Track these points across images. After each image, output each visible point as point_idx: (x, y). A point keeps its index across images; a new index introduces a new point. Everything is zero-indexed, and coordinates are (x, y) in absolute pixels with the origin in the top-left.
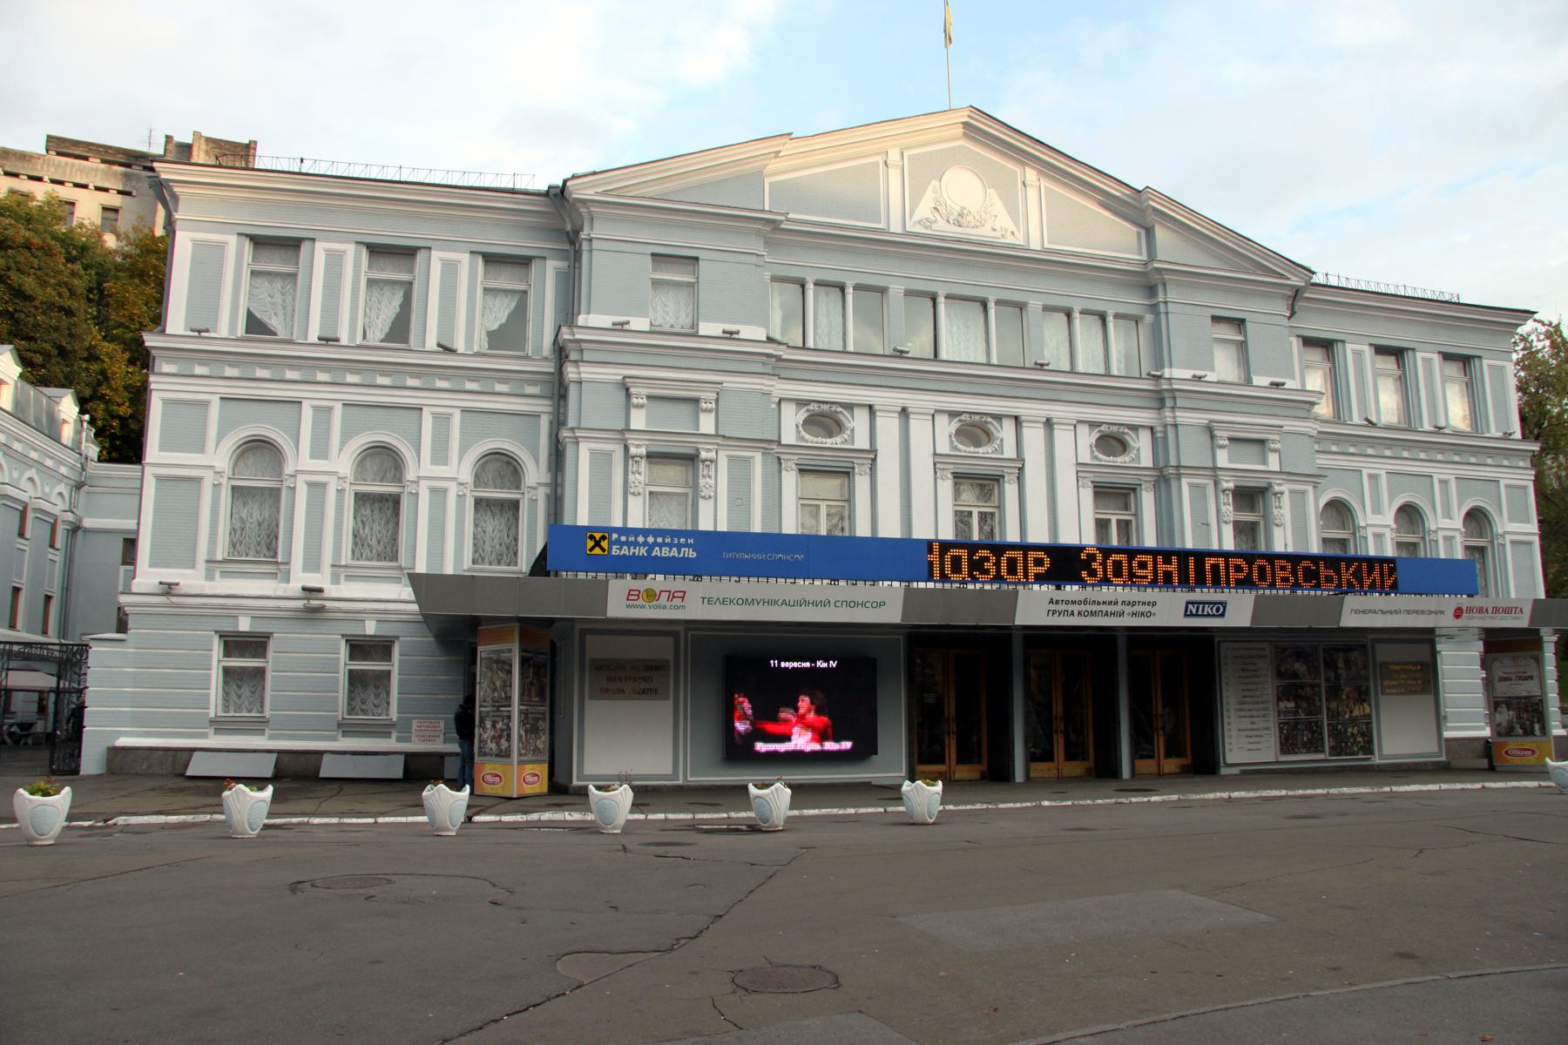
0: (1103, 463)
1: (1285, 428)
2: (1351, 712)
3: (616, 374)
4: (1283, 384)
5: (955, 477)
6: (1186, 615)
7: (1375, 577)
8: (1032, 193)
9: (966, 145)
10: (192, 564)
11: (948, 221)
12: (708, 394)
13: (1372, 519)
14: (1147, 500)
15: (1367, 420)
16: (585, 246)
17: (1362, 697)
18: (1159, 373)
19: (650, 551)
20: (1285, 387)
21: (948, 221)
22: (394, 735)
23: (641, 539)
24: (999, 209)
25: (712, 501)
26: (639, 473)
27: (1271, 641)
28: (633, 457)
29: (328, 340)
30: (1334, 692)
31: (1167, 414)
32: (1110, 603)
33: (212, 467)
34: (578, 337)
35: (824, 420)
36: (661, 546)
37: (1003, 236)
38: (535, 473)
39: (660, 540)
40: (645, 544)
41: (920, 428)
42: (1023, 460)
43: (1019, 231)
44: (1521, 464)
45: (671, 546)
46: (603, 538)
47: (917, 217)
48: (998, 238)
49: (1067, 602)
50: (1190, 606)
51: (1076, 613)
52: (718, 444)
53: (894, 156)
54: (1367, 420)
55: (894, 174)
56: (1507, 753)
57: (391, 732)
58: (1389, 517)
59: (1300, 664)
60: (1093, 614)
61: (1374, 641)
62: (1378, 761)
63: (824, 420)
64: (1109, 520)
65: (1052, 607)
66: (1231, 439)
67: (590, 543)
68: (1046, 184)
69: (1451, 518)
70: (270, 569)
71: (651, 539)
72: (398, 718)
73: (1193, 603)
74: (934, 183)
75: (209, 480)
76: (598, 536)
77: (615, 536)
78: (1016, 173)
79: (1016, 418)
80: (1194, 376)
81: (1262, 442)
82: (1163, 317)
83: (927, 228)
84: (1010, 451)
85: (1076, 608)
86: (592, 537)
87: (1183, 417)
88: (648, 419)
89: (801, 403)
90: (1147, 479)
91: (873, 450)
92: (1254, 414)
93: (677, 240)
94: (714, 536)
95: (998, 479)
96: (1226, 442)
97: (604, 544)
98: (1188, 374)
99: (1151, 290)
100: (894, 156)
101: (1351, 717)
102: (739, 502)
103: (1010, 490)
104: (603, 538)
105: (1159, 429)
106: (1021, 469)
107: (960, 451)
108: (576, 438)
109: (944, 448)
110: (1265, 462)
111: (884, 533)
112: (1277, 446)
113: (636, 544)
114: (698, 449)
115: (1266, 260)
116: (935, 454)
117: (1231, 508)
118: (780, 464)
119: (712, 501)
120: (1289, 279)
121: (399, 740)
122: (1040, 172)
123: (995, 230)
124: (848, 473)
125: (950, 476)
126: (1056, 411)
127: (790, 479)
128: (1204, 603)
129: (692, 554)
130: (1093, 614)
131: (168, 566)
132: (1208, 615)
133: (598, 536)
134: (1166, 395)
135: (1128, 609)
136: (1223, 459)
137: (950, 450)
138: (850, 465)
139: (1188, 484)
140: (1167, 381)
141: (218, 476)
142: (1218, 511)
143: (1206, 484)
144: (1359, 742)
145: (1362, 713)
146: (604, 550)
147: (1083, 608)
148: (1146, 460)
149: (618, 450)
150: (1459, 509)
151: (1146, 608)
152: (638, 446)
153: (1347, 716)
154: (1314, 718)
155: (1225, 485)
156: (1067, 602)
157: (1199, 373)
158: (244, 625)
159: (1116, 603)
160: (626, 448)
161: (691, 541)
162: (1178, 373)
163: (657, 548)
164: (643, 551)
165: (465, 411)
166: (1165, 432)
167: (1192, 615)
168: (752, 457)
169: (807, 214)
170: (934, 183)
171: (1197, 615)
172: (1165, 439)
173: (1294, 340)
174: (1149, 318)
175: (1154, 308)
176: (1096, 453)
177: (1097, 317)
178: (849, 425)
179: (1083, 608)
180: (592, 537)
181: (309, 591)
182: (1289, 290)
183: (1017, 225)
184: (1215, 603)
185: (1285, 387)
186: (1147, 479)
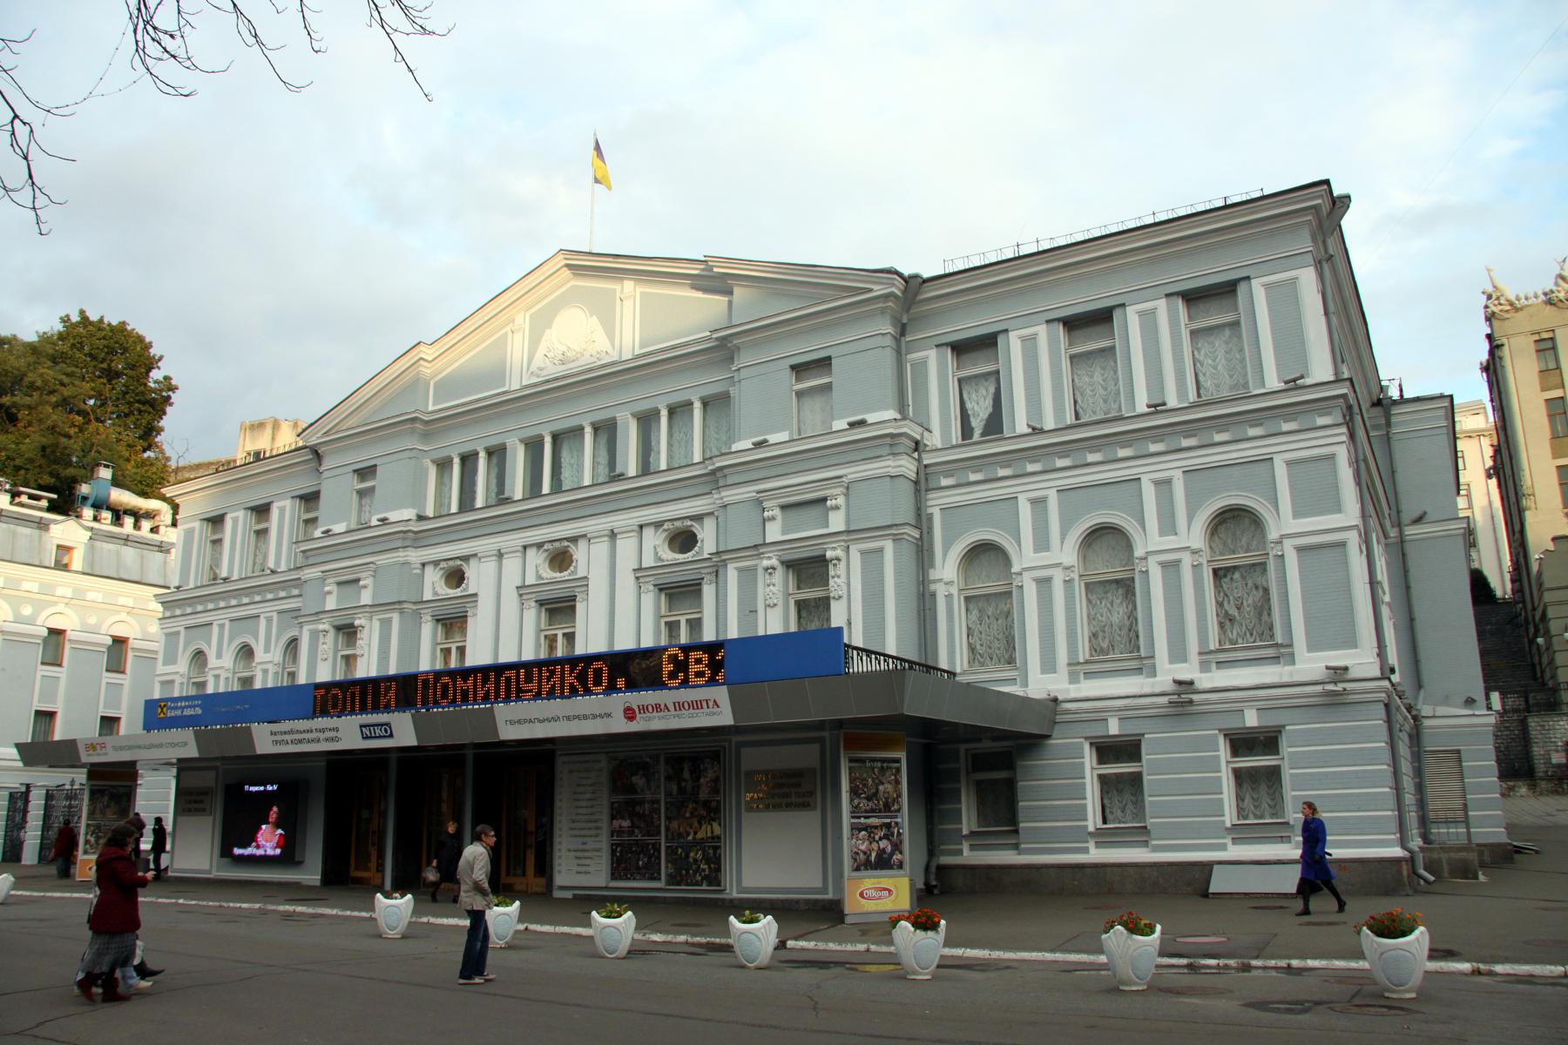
0: (666, 563)
2: (695, 833)
7: (555, 683)
17: (712, 812)
23: (179, 704)
27: (607, 753)
30: (676, 809)
32: (308, 731)
33: (177, 673)
45: (190, 707)
48: (595, 362)
50: (364, 729)
52: (370, 612)
56: (861, 895)
59: (639, 777)
60: (300, 741)
61: (740, 745)
62: (735, 895)
64: (679, 621)
66: (783, 507)
69: (1176, 534)
73: (365, 726)
75: (178, 680)
81: (824, 500)
83: (538, 377)
86: (160, 706)
88: (339, 600)
92: (740, 483)
93: (362, 457)
94: (216, 695)
98: (747, 444)
101: (694, 838)
104: (165, 706)
120: (871, 290)
125: (533, 604)
126: (619, 521)
127: (427, 630)
129: (199, 711)
130: (300, 741)
132: (380, 737)
135: (322, 736)
138: (461, 610)
144: (704, 870)
145: (709, 835)
150: (1190, 518)
153: (690, 838)
154: (650, 840)
159: (312, 731)
165: (280, 612)
168: (391, 618)
169: (457, 399)
184: (382, 725)
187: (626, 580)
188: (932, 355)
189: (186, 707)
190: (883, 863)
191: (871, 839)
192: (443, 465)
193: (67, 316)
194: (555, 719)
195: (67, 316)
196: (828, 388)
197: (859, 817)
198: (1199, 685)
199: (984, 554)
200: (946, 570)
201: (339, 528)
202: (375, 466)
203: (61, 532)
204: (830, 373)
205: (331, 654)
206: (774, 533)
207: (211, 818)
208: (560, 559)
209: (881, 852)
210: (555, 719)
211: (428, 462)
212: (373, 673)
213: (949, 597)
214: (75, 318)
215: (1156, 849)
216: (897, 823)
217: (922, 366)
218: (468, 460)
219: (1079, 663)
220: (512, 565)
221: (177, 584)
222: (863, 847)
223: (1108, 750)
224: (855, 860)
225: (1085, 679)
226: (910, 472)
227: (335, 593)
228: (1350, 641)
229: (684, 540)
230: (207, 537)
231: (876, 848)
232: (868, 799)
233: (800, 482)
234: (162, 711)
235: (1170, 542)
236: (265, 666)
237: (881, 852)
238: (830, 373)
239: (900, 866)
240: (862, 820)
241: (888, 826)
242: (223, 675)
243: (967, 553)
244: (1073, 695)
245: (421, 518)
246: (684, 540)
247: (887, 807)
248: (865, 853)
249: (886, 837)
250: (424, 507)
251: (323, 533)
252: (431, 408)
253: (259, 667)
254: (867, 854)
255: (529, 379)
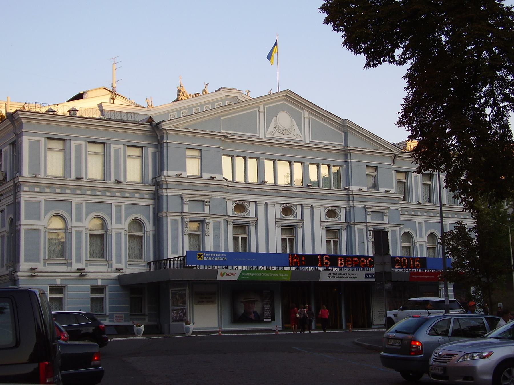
3: (178, 192)
4: (390, 191)
5: (281, 226)
6: (365, 278)
8: (306, 120)
9: (285, 103)
10: (38, 261)
11: (279, 132)
12: (207, 199)
13: (419, 239)
14: (343, 233)
15: (418, 202)
16: (165, 145)
18: (348, 188)
19: (214, 259)
20: (391, 192)
21: (279, 132)
22: (108, 319)
23: (212, 255)
24: (296, 127)
25: (209, 236)
26: (187, 228)
28: (185, 222)
29: (79, 179)
31: (351, 203)
32: (345, 274)
34: (167, 180)
35: (240, 207)
36: (217, 257)
37: (297, 138)
38: (149, 226)
39: (217, 255)
40: (213, 256)
41: (270, 209)
42: (304, 220)
43: (302, 135)
45: (220, 257)
46: (202, 255)
47: (269, 131)
49: (333, 274)
51: (335, 277)
53: (261, 108)
54: (418, 202)
55: (261, 115)
57: (106, 319)
58: (425, 239)
60: (340, 277)
63: (240, 207)
65: (329, 276)
67: (198, 256)
68: (312, 117)
70: (64, 262)
71: (214, 255)
72: (109, 314)
73: (367, 274)
74: (275, 118)
76: (200, 254)
77: (205, 254)
78: (301, 113)
79: (301, 205)
80: (360, 189)
82: (350, 166)
84: (299, 217)
85: (335, 276)
86: (199, 255)
87: (356, 204)
89: (234, 201)
90: (343, 226)
91: (256, 217)
95: (295, 227)
96: (370, 213)
97: (202, 256)
99: (346, 156)
100: (261, 108)
102: (217, 237)
103: (299, 231)
104: (202, 255)
105: (348, 208)
106: (303, 223)
107: (283, 217)
108: (167, 215)
109: (278, 216)
110: (383, 220)
111: (272, 251)
112: (387, 214)
113: (210, 256)
114: (205, 219)
115: (386, 145)
116: (276, 219)
117: (372, 237)
118: (227, 223)
119: (209, 236)
121: (110, 321)
122: (309, 113)
123: (294, 135)
124: (248, 225)
128: (370, 274)
130: (340, 277)
131: (30, 262)
132: (371, 278)
133: (200, 254)
134: (351, 196)
135: (349, 276)
136: (369, 219)
137: (280, 217)
139: (357, 228)
140: (351, 192)
141: (45, 228)
142: (367, 238)
143: (363, 228)
146: (202, 258)
147: (337, 276)
148: (343, 220)
149: (179, 218)
151: (355, 276)
152: (187, 218)
155: (370, 229)
156: (333, 274)
157: (361, 188)
158: (58, 282)
159: (346, 274)
160: (182, 219)
161: (225, 255)
162: (354, 188)
163: (216, 258)
164: (212, 258)
165: (126, 204)
166: (350, 210)
167: (367, 278)
170: (275, 118)
171: (368, 278)
172: (350, 211)
173: (393, 172)
174: (345, 166)
175: (346, 163)
176: (327, 217)
177: (326, 166)
178: (249, 209)
179: (337, 276)
180: (199, 255)
181: (79, 270)
182: (393, 155)
183: (301, 133)
185: (391, 192)
186: (343, 226)
207: (216, 305)
234: (200, 257)
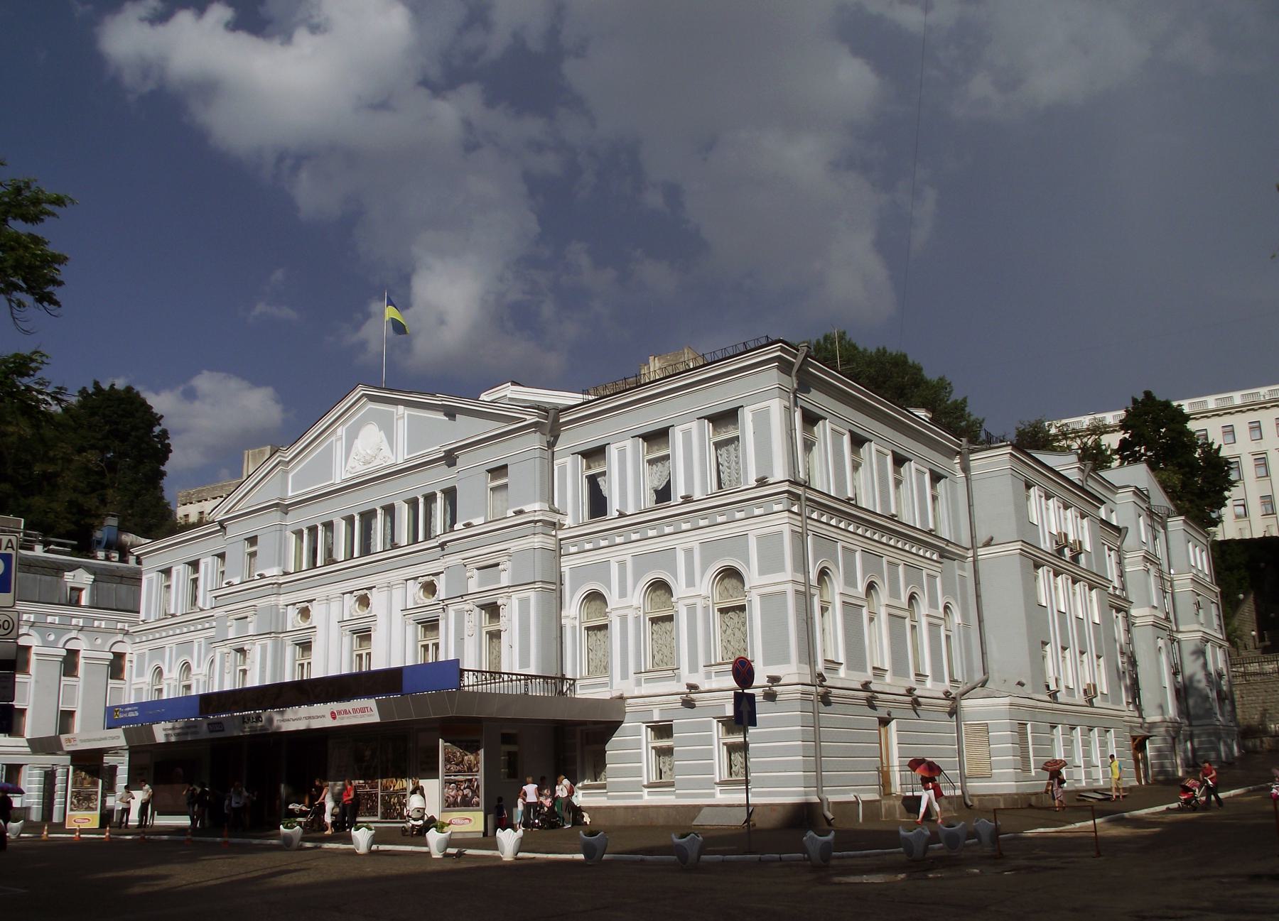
1: (512, 549)
2: (394, 786)
44: (776, 508)
75: (145, 689)
81: (497, 565)
101: (394, 790)
120: (525, 420)
125: (348, 633)
129: (137, 714)
144: (398, 810)
145: (401, 787)
153: (392, 789)
154: (373, 791)
187: (397, 616)
188: (569, 461)
189: (130, 711)
190: (466, 803)
191: (458, 789)
192: (299, 533)
193: (84, 388)
194: (105, 739)
195: (84, 388)
196: (505, 486)
197: (451, 776)
198: (702, 689)
199: (595, 597)
200: (573, 610)
201: (236, 580)
202: (256, 536)
203: (72, 577)
204: (506, 475)
205: (233, 668)
206: (473, 586)
208: (364, 601)
209: (465, 796)
210: (105, 739)
211: (288, 533)
212: (256, 684)
213: (574, 628)
214: (91, 390)
215: (678, 796)
216: (476, 779)
217: (563, 468)
218: (313, 530)
219: (641, 673)
220: (335, 606)
221: (143, 619)
222: (453, 794)
223: (663, 730)
224: (447, 801)
225: (645, 683)
226: (551, 546)
227: (234, 626)
228: (785, 660)
229: (430, 588)
230: (161, 584)
231: (461, 794)
232: (457, 764)
233: (484, 552)
235: (692, 592)
236: (197, 677)
237: (465, 796)
238: (506, 475)
239: (478, 804)
240: (452, 777)
241: (470, 781)
242: (173, 683)
243: (584, 599)
244: (636, 693)
245: (286, 574)
246: (430, 588)
247: (470, 769)
248: (453, 797)
249: (468, 787)
250: (285, 564)
251: (226, 584)
252: (290, 494)
253: (194, 677)
254: (455, 797)
255: (345, 475)
